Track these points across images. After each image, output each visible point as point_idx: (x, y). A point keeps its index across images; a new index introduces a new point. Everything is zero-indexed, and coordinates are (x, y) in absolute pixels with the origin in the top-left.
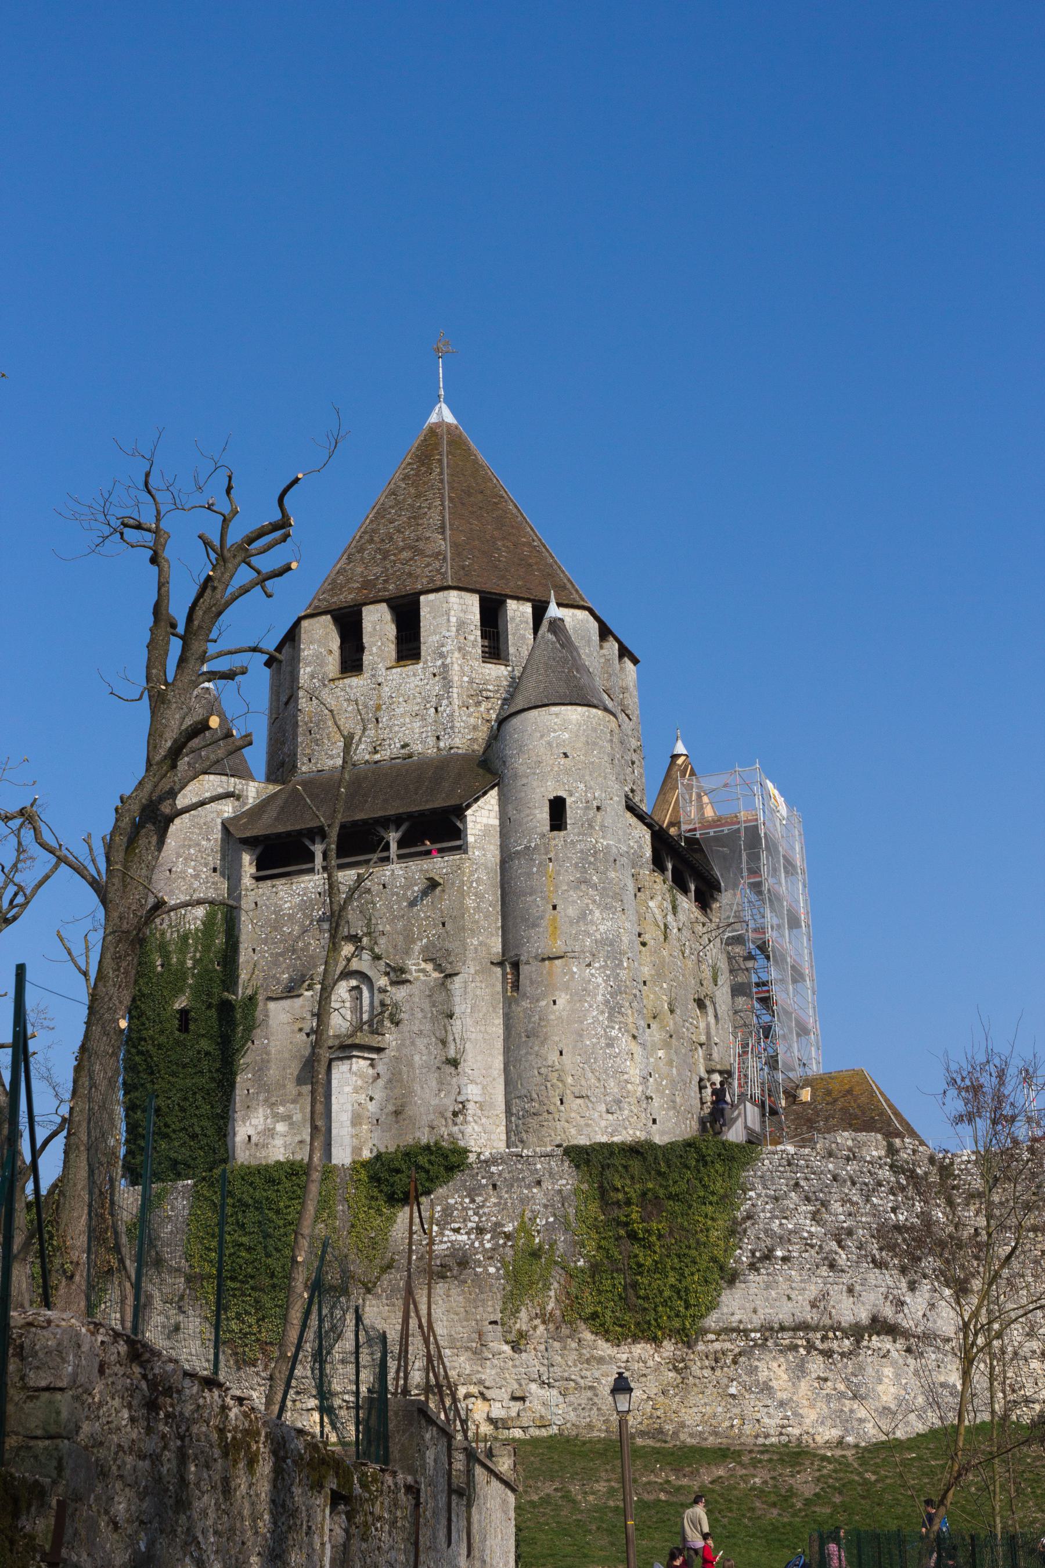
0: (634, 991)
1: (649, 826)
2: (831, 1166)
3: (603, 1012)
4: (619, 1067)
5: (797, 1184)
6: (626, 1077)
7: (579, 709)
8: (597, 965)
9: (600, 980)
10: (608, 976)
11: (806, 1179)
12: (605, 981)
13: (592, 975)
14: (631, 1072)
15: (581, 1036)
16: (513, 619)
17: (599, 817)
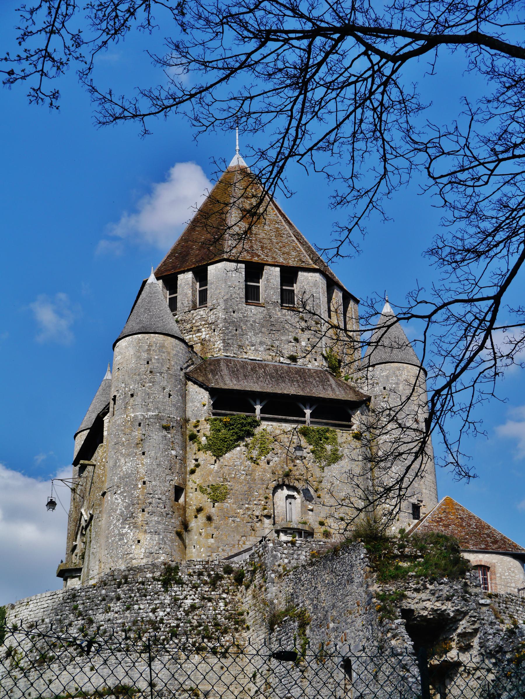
0: (150, 500)
1: (206, 389)
2: (104, 592)
3: (119, 520)
4: (126, 551)
5: (76, 608)
6: (131, 556)
7: (127, 338)
8: (119, 492)
9: (120, 501)
10: (125, 497)
11: (83, 604)
12: (122, 500)
13: (116, 499)
14: (136, 552)
15: (107, 537)
16: (181, 284)
17: (132, 400)
